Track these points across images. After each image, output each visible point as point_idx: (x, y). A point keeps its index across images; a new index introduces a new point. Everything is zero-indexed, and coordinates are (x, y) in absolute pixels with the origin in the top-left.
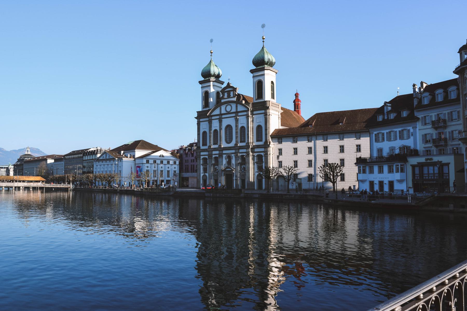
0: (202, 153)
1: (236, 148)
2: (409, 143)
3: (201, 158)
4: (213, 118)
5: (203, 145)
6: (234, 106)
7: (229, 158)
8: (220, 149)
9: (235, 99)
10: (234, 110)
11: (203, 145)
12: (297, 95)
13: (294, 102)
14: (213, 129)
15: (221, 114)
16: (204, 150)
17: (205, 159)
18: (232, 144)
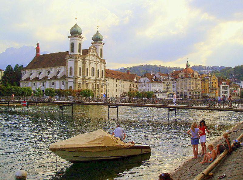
0: (78, 80)
1: (96, 80)
2: (160, 88)
3: (78, 83)
4: (86, 61)
5: (79, 75)
6: (95, 57)
7: (93, 84)
8: (89, 79)
9: (95, 54)
10: (95, 60)
11: (79, 75)
12: (38, 45)
13: (36, 48)
14: (86, 68)
15: (89, 60)
16: (80, 79)
17: (80, 84)
18: (94, 78)
